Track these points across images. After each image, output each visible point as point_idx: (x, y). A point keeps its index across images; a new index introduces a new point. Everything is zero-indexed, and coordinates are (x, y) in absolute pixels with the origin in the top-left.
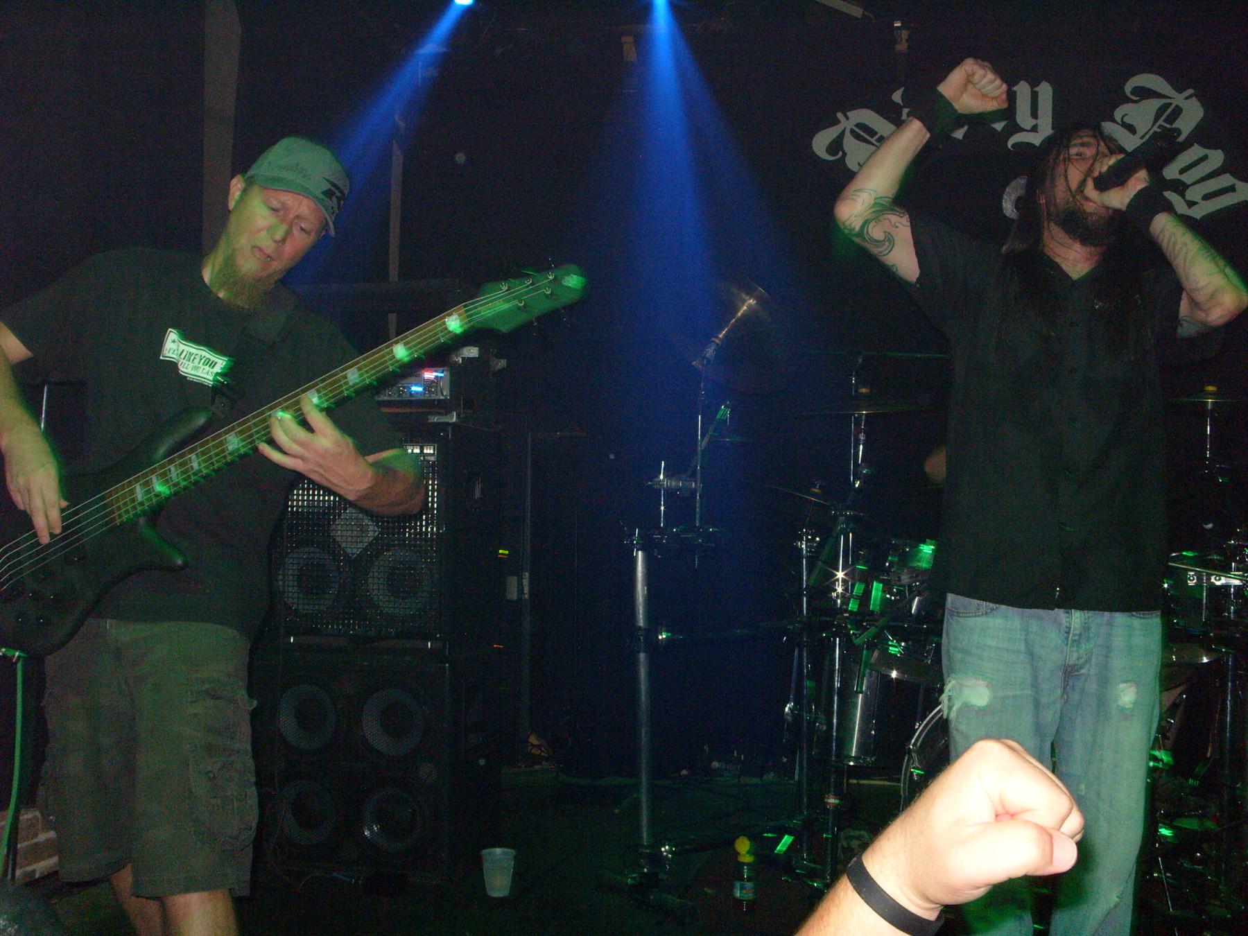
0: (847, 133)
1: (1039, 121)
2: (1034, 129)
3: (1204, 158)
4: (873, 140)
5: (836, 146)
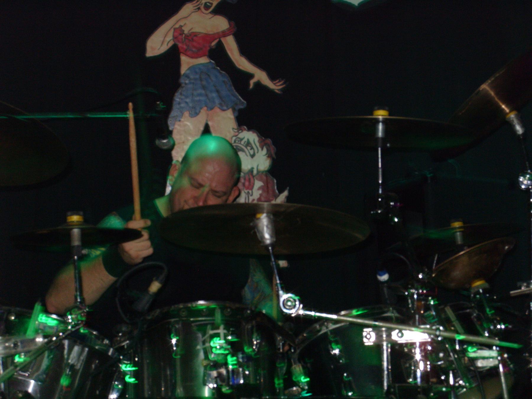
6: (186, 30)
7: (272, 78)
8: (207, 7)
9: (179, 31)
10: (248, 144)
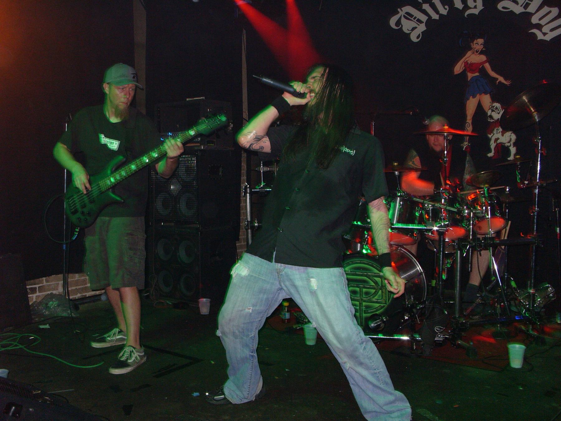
0: (403, 18)
1: (477, 4)
2: (475, 7)
3: (550, 12)
4: (412, 19)
5: (398, 23)
6: (469, 62)
7: (506, 79)
8: (477, 52)
9: (466, 63)
10: (497, 108)
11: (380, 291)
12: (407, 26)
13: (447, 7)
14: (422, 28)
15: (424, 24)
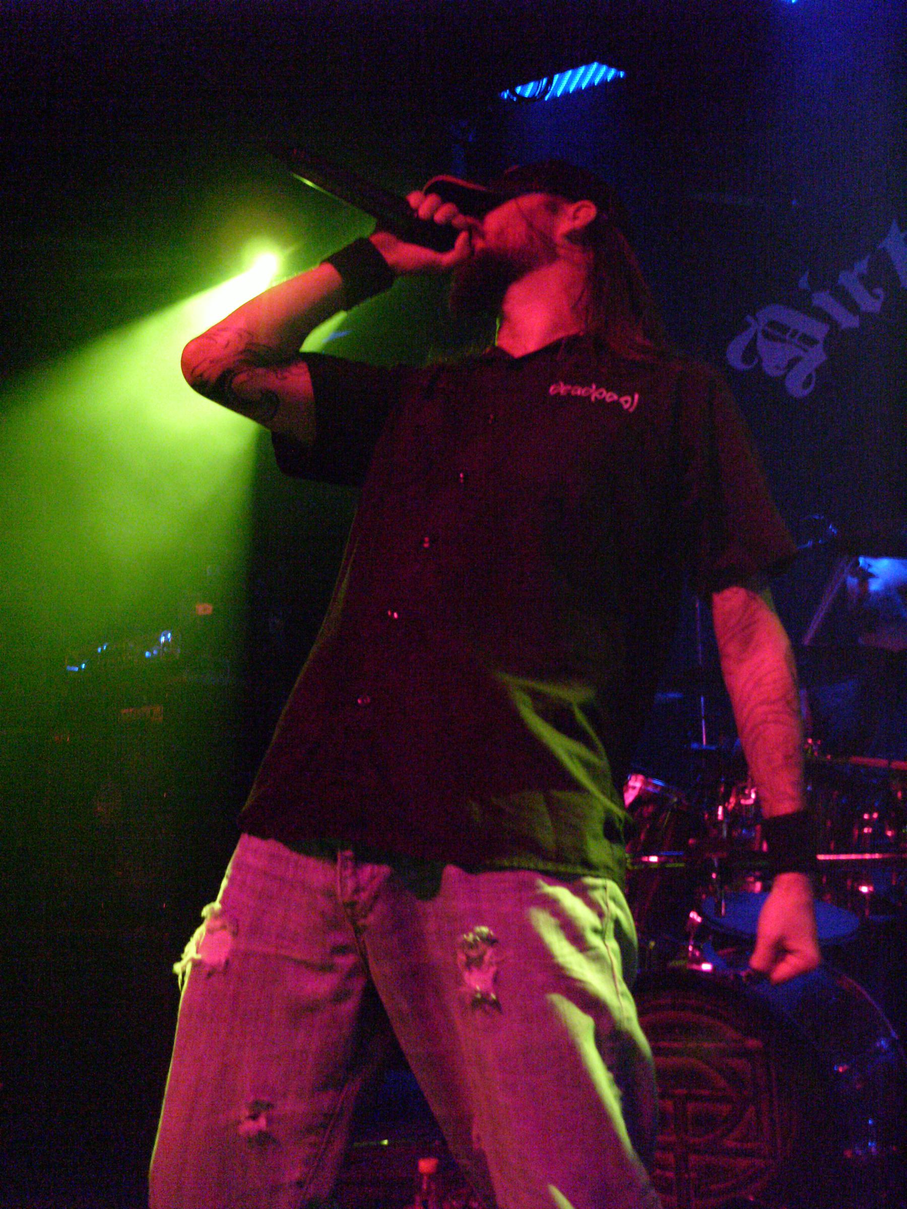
0: (759, 335)
5: (751, 352)
11: (751, 1110)
12: (773, 358)
13: (879, 291)
14: (816, 357)
15: (820, 346)
